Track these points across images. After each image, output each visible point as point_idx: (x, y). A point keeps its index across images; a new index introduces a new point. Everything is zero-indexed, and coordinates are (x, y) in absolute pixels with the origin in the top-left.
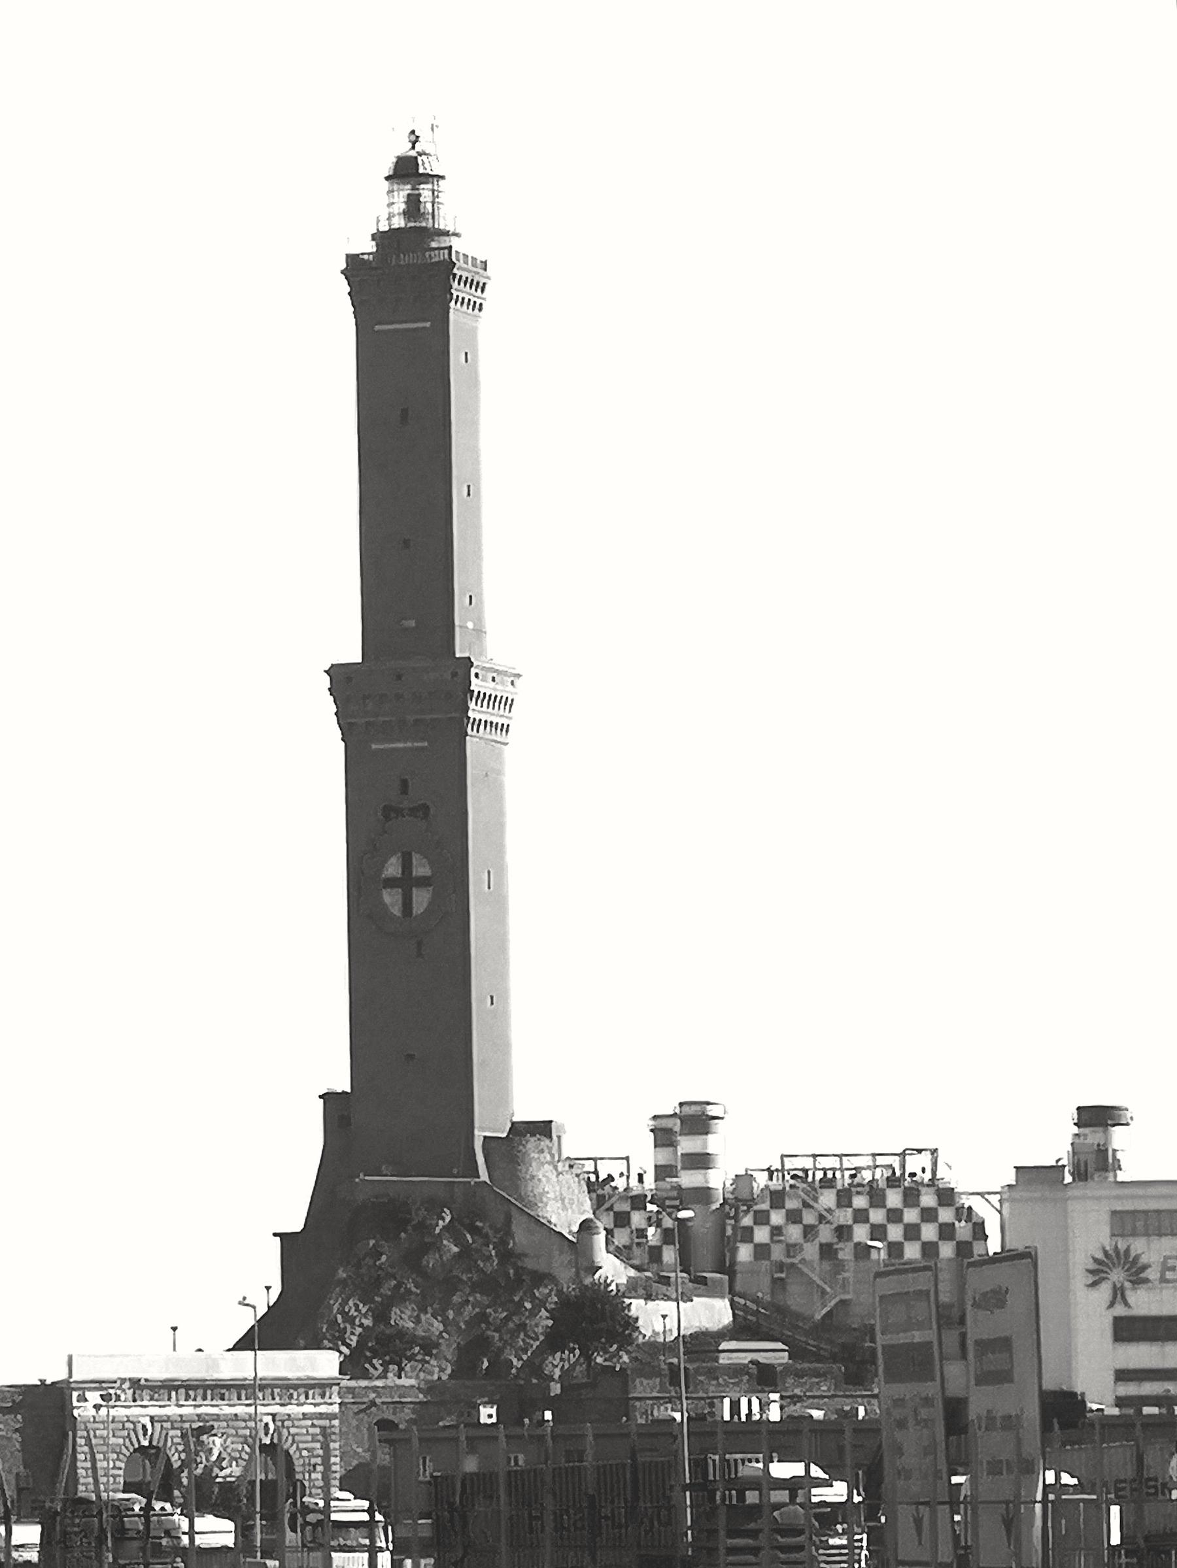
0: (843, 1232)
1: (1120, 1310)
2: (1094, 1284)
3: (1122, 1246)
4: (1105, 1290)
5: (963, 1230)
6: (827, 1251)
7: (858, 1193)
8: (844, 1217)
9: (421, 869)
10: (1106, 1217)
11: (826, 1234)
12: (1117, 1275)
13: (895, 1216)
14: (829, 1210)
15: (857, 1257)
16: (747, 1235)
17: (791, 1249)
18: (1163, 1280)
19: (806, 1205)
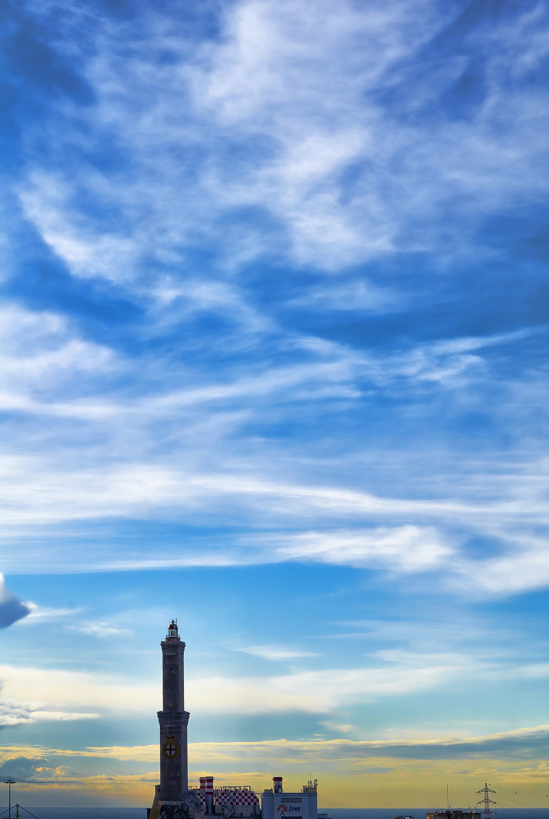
0: (234, 800)
5: (255, 800)
6: (231, 804)
8: (235, 797)
9: (173, 747)
11: (231, 801)
12: (282, 809)
13: (243, 797)
17: (225, 803)
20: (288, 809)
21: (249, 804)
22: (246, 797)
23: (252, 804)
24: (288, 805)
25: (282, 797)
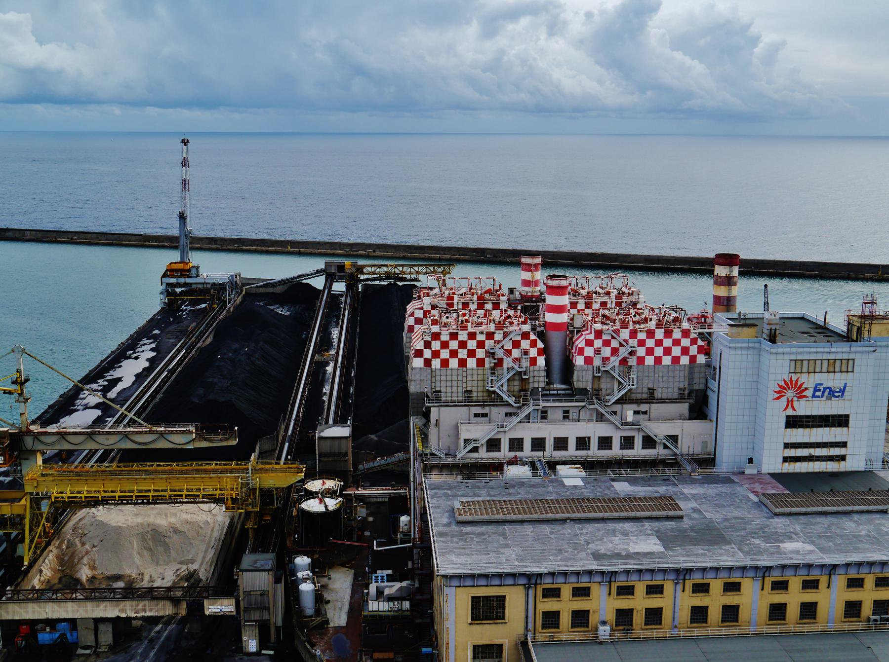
1: (789, 412)
2: (778, 398)
3: (794, 378)
4: (784, 400)
6: (624, 362)
10: (787, 363)
11: (623, 352)
12: (790, 394)
14: (625, 341)
15: (638, 363)
16: (581, 351)
17: (606, 360)
18: (814, 396)
19: (613, 338)
20: (809, 393)
21: (676, 360)
22: (668, 343)
23: (685, 360)
24: (809, 381)
25: (794, 357)
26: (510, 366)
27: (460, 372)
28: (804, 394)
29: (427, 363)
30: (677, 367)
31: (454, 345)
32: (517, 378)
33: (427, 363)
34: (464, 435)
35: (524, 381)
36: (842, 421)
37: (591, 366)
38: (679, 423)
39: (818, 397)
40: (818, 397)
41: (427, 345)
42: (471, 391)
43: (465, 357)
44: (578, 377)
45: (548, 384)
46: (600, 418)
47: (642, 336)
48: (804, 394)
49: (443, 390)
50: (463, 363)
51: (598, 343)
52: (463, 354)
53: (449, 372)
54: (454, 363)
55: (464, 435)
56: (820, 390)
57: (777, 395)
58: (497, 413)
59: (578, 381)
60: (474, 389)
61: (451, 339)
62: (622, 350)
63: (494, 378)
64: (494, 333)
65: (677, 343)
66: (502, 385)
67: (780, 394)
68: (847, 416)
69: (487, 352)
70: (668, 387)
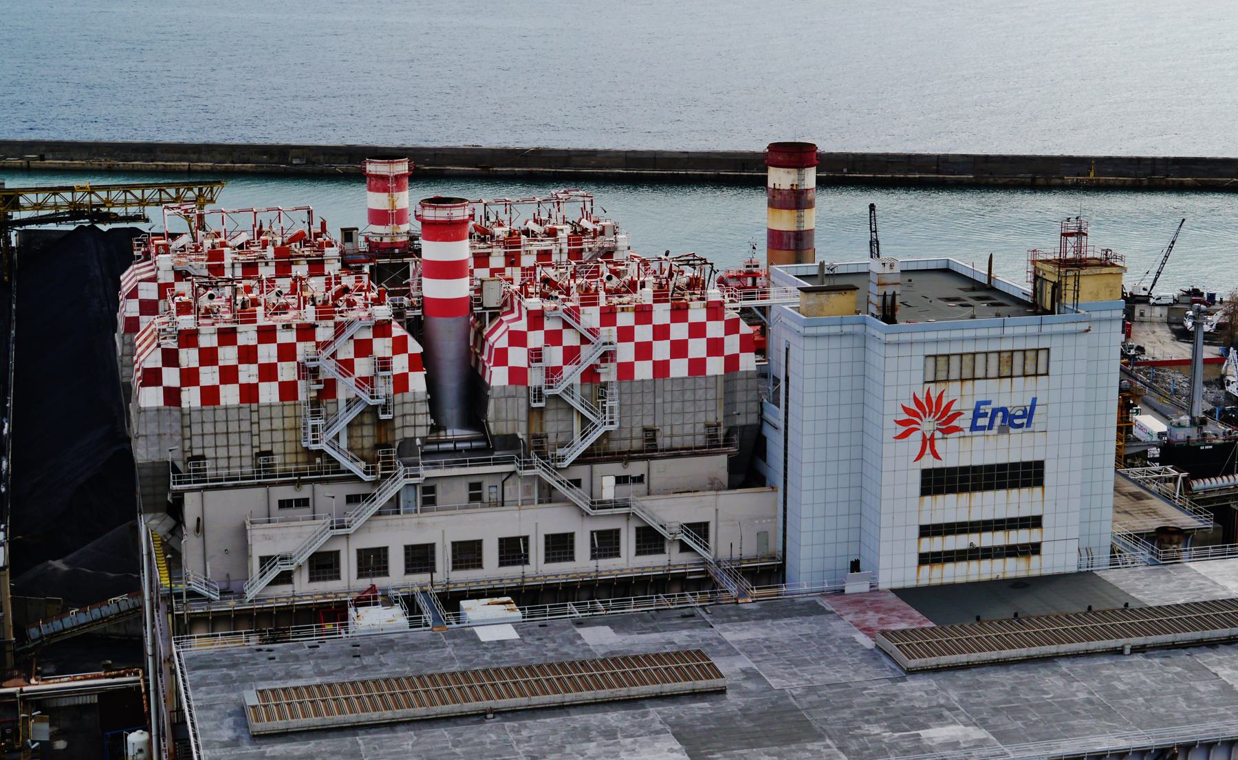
1: (929, 462)
2: (904, 435)
6: (590, 375)
7: (623, 310)
11: (589, 355)
12: (928, 425)
14: (593, 331)
15: (620, 378)
16: (501, 357)
18: (974, 427)
19: (566, 325)
20: (964, 422)
21: (697, 367)
22: (679, 331)
23: (715, 366)
24: (962, 397)
26: (352, 396)
27: (245, 413)
28: (955, 423)
29: (172, 396)
30: (700, 381)
31: (228, 355)
32: (367, 419)
33: (172, 396)
34: (259, 548)
35: (384, 427)
36: (1028, 475)
37: (522, 389)
38: (710, 496)
39: (983, 428)
40: (983, 428)
41: (170, 358)
42: (270, 453)
43: (254, 380)
44: (497, 411)
45: (436, 428)
46: (548, 495)
47: (626, 319)
48: (955, 423)
49: (209, 453)
50: (249, 394)
51: (536, 339)
52: (248, 373)
53: (221, 415)
54: (230, 395)
55: (259, 548)
56: (985, 415)
57: (902, 429)
58: (329, 496)
59: (497, 420)
60: (278, 448)
61: (222, 342)
62: (585, 350)
63: (320, 422)
64: (314, 327)
65: (697, 330)
66: (337, 437)
67: (908, 426)
68: (1040, 465)
69: (302, 368)
70: (686, 421)
